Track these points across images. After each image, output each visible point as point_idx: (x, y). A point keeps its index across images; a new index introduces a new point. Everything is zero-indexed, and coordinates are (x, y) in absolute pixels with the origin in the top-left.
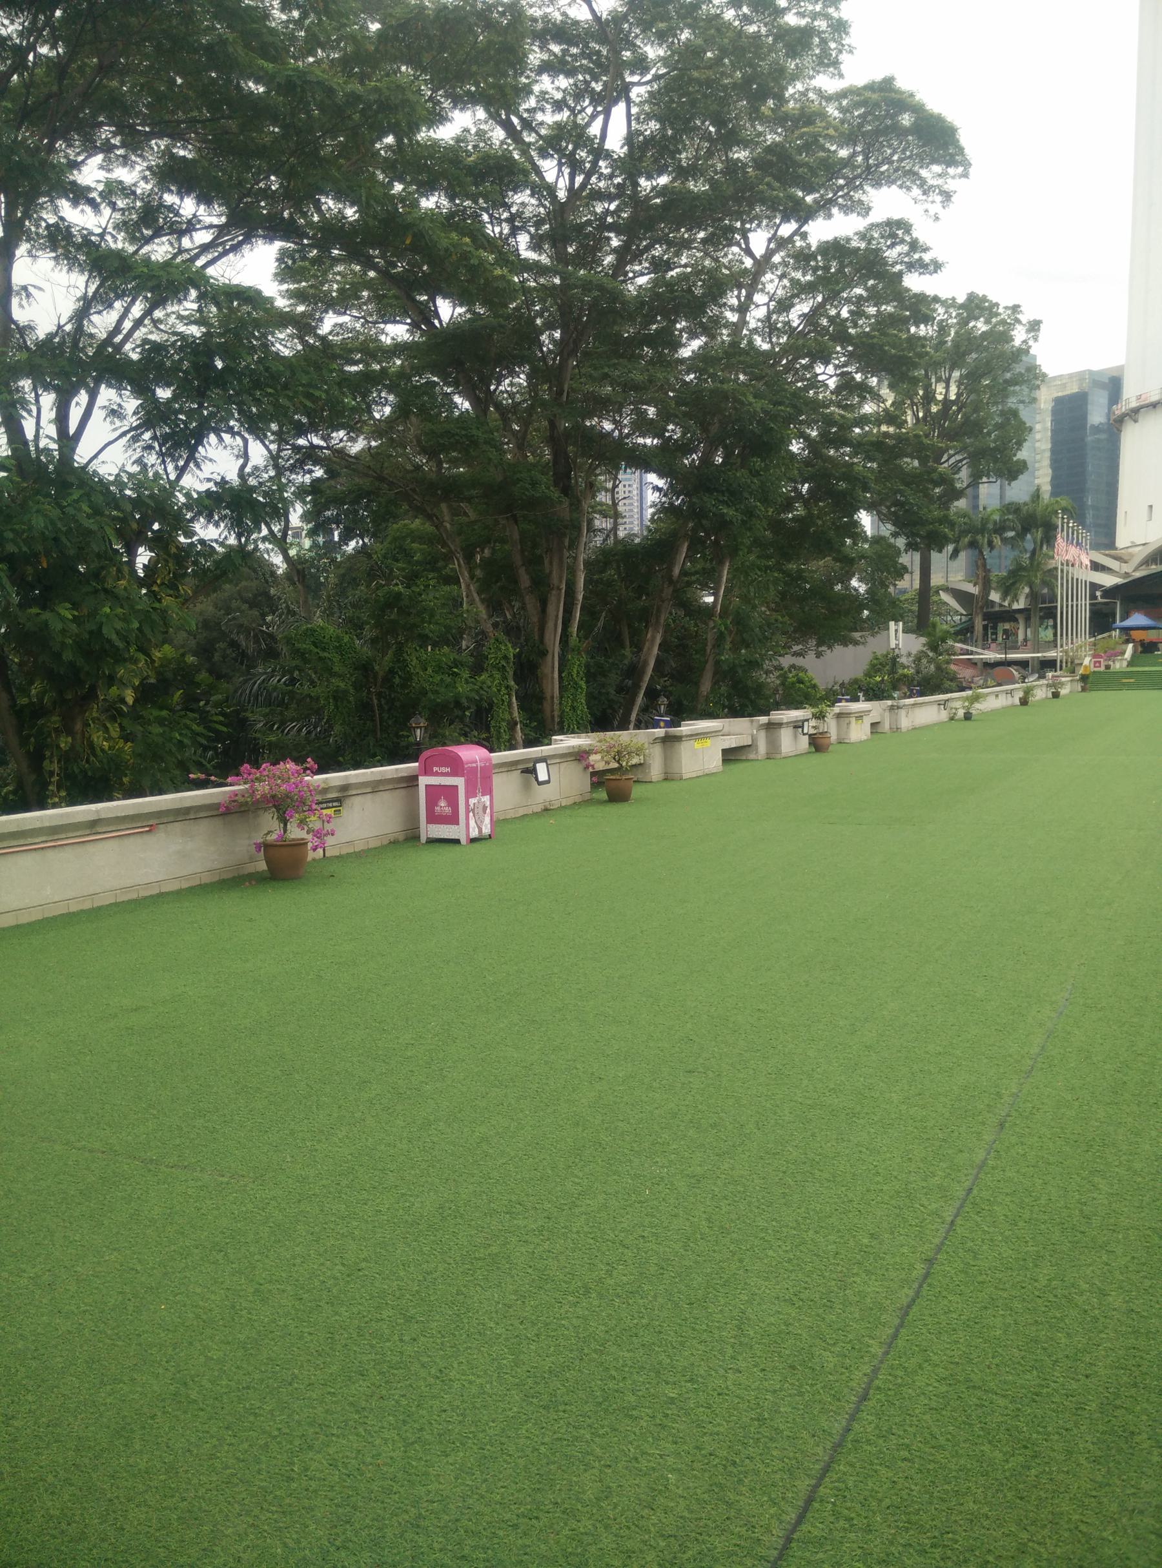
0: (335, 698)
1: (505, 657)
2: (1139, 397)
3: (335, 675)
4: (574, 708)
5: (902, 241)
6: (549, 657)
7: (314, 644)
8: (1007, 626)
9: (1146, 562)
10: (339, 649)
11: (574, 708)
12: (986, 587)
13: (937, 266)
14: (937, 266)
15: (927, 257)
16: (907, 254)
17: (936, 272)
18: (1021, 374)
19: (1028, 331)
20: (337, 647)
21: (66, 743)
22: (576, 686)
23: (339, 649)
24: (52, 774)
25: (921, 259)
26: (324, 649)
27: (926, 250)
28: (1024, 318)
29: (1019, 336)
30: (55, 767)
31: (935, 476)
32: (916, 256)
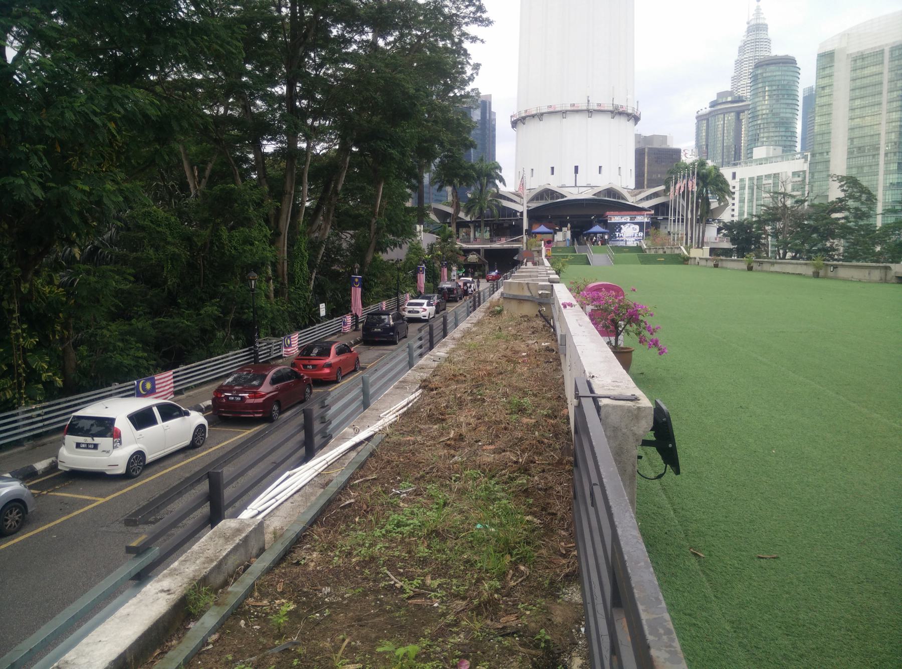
0: (171, 259)
1: (265, 236)
2: (526, 111)
3: (168, 243)
4: (301, 270)
5: (474, 5)
6: (282, 237)
7: (152, 222)
8: (464, 230)
9: (532, 200)
10: (169, 226)
11: (301, 270)
12: (457, 210)
13: (488, 22)
14: (488, 22)
15: (484, 16)
16: (474, 13)
17: (487, 25)
18: (468, 93)
19: (473, 69)
20: (166, 225)
21: (25, 288)
22: (303, 256)
23: (169, 226)
24: (11, 312)
25: (481, 16)
26: (159, 226)
27: (484, 12)
28: (472, 62)
29: (469, 71)
30: (15, 306)
31: (467, 142)
32: (479, 14)
